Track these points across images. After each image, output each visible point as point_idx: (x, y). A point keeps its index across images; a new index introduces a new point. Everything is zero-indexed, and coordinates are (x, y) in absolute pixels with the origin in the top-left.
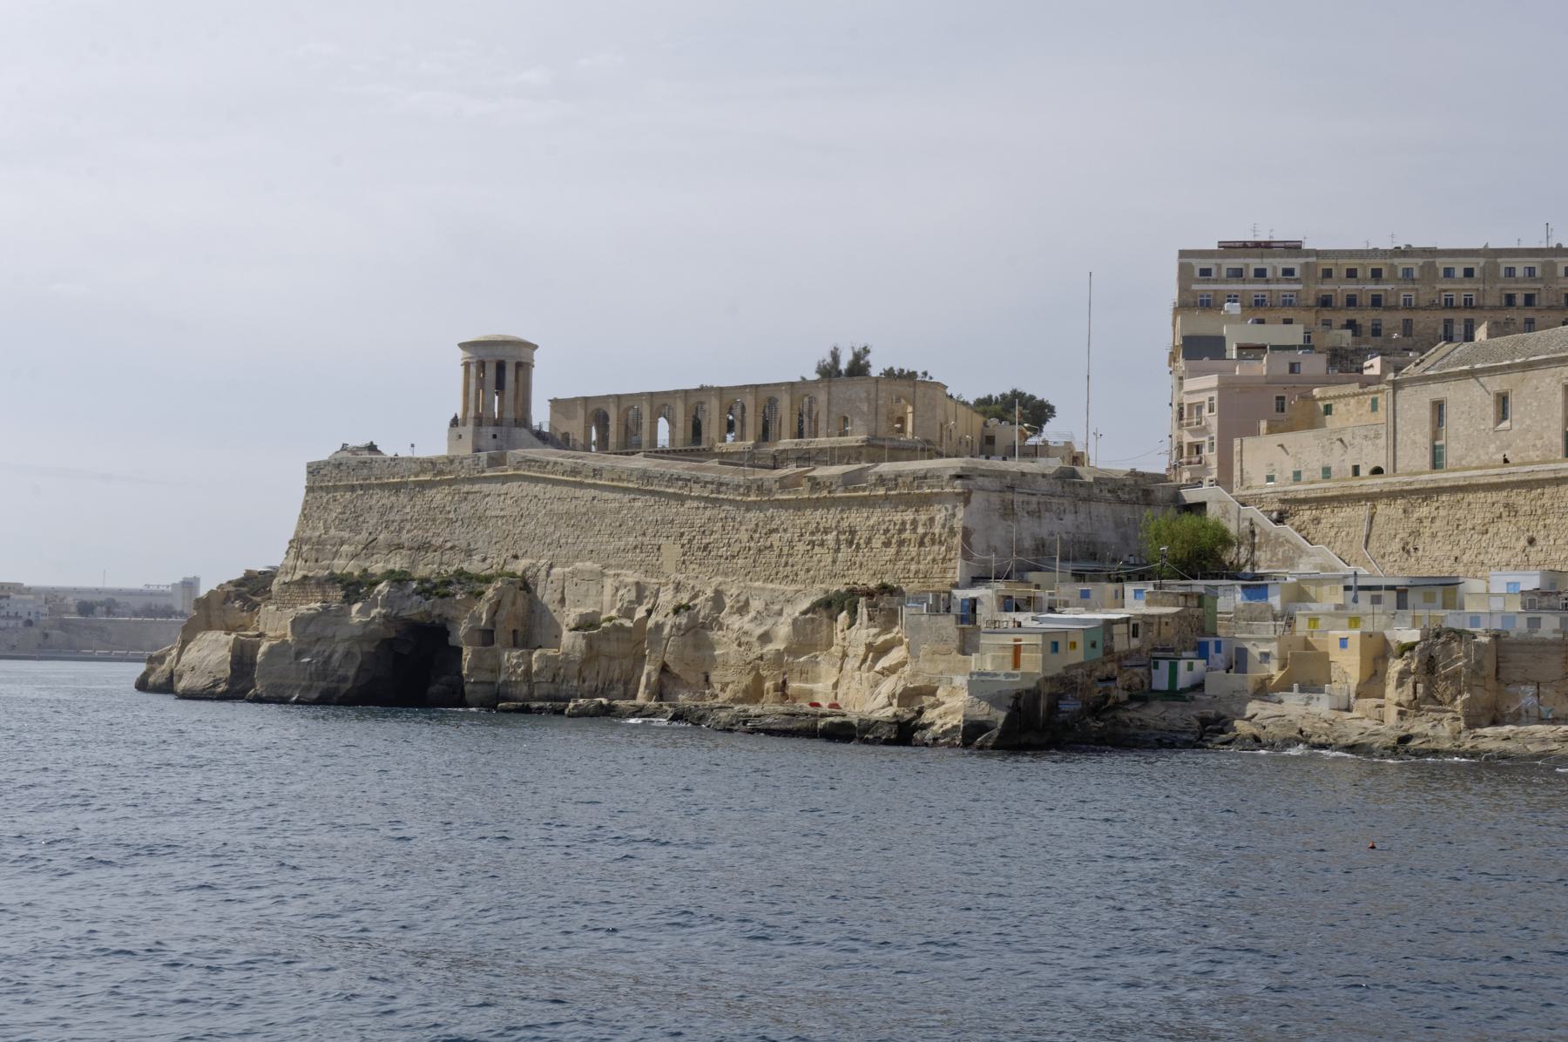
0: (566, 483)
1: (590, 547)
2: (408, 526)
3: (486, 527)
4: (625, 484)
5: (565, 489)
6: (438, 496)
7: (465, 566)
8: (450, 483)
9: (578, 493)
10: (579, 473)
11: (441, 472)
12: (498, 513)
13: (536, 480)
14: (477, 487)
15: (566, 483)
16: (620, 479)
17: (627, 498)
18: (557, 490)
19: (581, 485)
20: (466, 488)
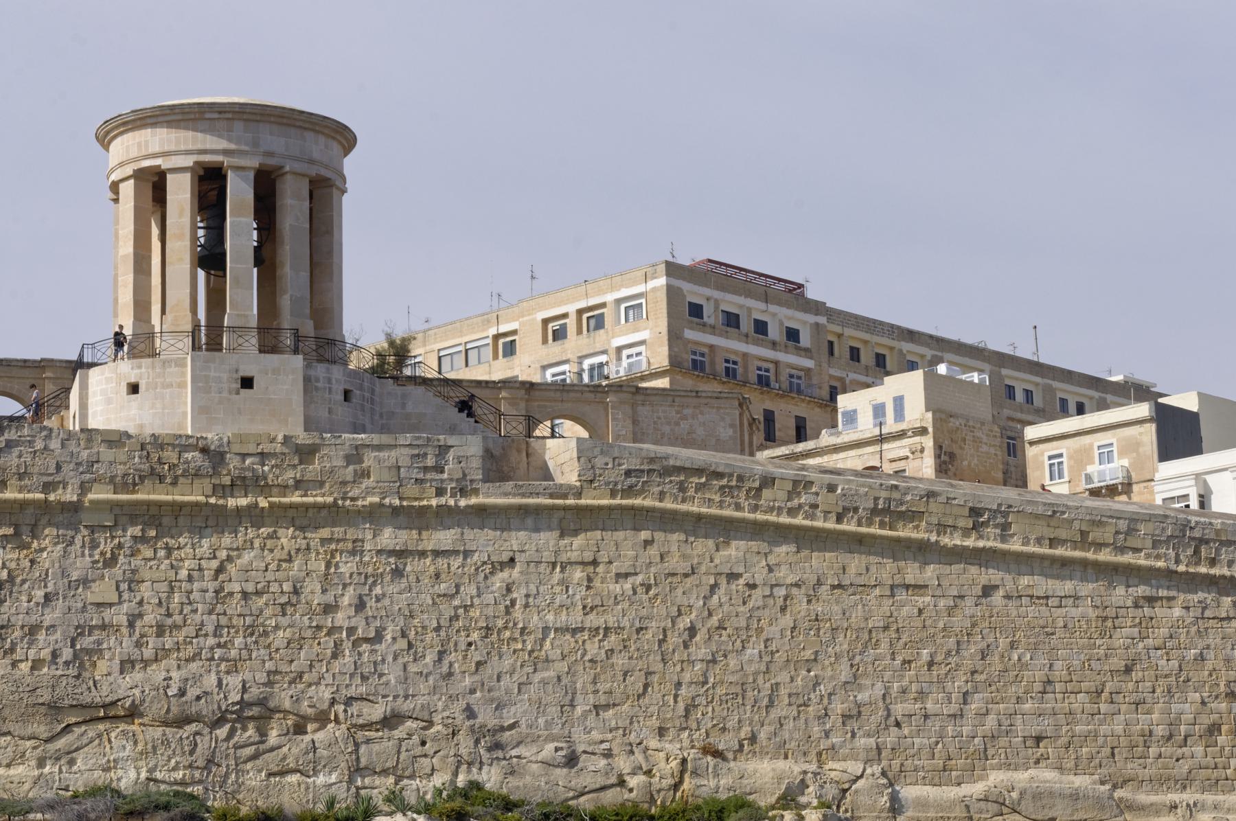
0: (859, 543)
1: (1022, 728)
2: (119, 646)
3: (538, 662)
4: (1105, 556)
5: (856, 563)
6: (253, 557)
7: (491, 778)
8: (304, 519)
9: (912, 572)
10: (912, 516)
11: (240, 484)
12: (576, 618)
13: (725, 529)
14: (444, 538)
15: (859, 543)
16: (1083, 541)
17: (1120, 594)
18: (821, 562)
19: (922, 551)
20: (389, 537)
